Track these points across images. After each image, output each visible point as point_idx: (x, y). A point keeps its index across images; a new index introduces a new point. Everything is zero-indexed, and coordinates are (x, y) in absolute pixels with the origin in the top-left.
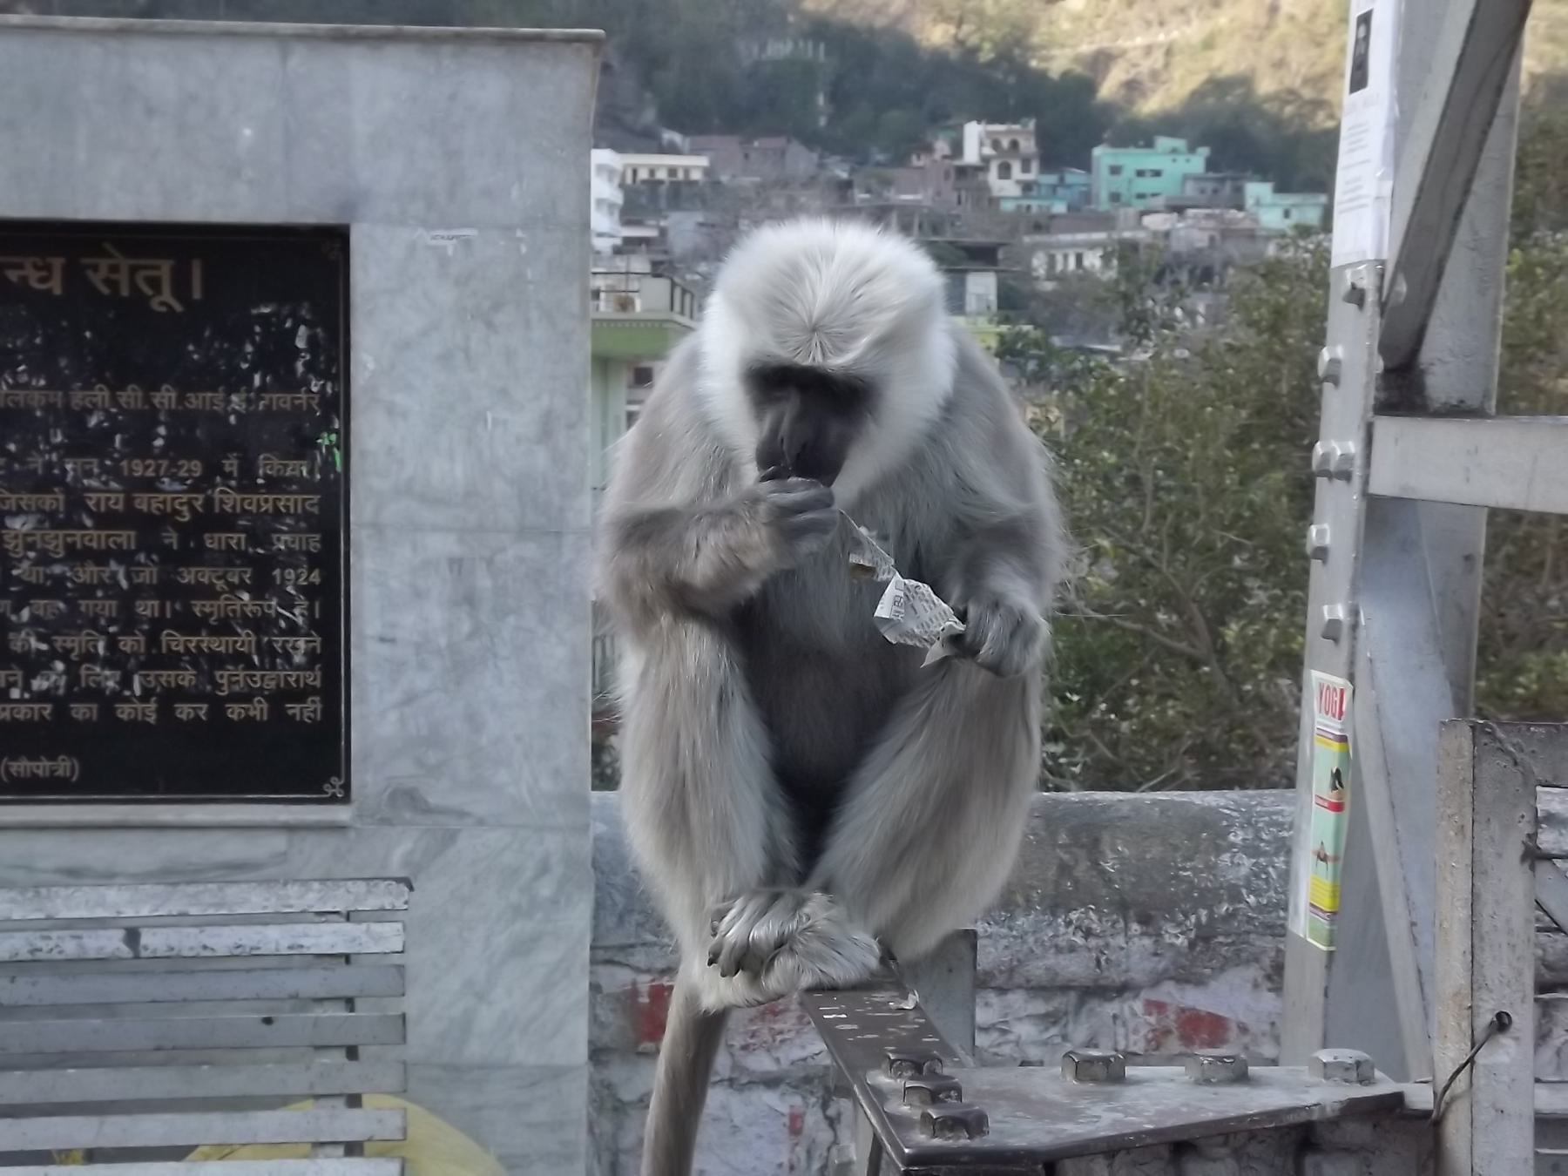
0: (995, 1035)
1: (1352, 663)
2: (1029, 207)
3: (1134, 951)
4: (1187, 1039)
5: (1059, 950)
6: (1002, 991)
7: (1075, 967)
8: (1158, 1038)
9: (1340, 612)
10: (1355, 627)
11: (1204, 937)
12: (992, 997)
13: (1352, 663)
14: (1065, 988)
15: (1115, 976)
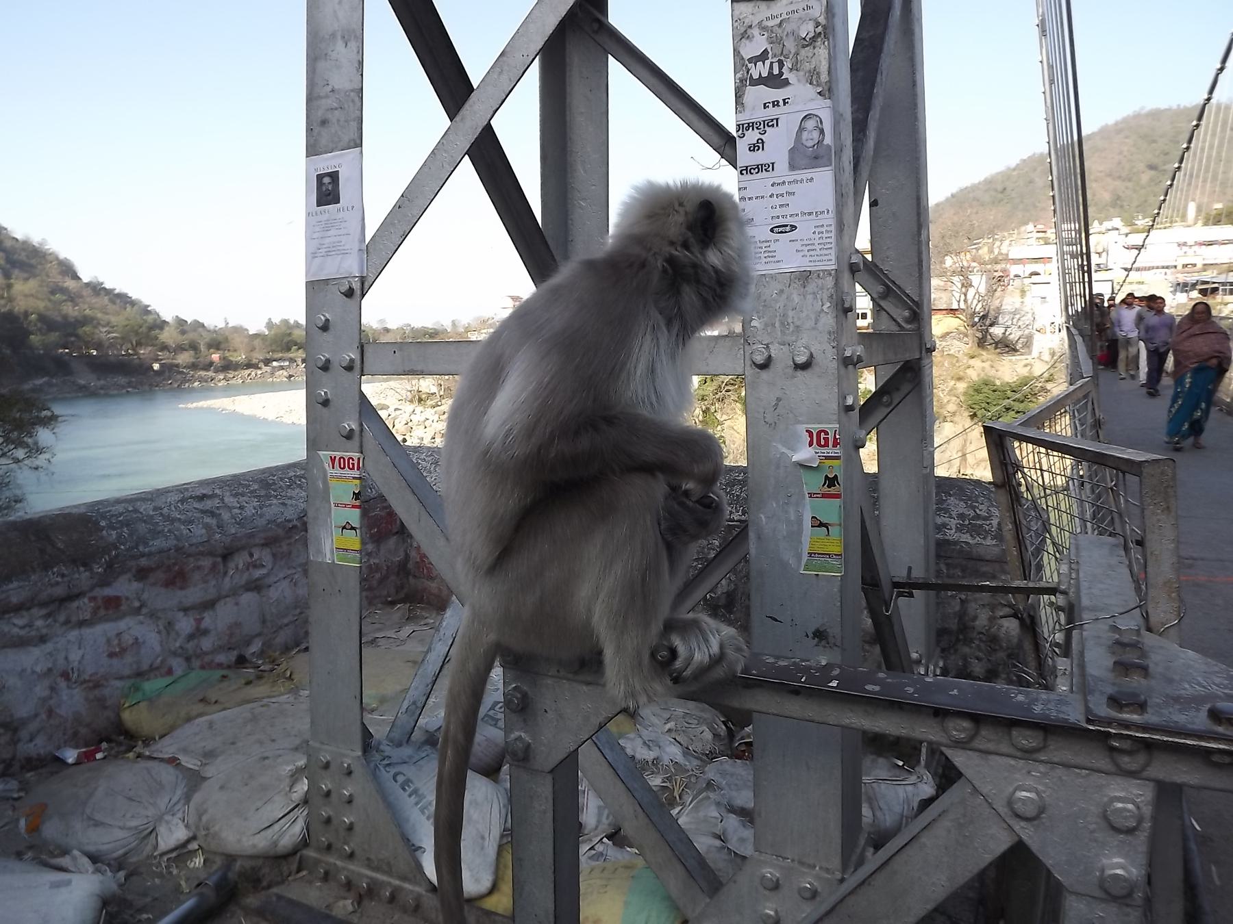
0: (27, 629)
1: (361, 446)
2: (1101, 224)
3: (83, 578)
4: (107, 608)
5: (52, 586)
6: (29, 609)
7: (59, 591)
8: (95, 611)
10: (362, 430)
11: (110, 566)
12: (25, 613)
13: (361, 446)
14: (53, 601)
15: (76, 591)
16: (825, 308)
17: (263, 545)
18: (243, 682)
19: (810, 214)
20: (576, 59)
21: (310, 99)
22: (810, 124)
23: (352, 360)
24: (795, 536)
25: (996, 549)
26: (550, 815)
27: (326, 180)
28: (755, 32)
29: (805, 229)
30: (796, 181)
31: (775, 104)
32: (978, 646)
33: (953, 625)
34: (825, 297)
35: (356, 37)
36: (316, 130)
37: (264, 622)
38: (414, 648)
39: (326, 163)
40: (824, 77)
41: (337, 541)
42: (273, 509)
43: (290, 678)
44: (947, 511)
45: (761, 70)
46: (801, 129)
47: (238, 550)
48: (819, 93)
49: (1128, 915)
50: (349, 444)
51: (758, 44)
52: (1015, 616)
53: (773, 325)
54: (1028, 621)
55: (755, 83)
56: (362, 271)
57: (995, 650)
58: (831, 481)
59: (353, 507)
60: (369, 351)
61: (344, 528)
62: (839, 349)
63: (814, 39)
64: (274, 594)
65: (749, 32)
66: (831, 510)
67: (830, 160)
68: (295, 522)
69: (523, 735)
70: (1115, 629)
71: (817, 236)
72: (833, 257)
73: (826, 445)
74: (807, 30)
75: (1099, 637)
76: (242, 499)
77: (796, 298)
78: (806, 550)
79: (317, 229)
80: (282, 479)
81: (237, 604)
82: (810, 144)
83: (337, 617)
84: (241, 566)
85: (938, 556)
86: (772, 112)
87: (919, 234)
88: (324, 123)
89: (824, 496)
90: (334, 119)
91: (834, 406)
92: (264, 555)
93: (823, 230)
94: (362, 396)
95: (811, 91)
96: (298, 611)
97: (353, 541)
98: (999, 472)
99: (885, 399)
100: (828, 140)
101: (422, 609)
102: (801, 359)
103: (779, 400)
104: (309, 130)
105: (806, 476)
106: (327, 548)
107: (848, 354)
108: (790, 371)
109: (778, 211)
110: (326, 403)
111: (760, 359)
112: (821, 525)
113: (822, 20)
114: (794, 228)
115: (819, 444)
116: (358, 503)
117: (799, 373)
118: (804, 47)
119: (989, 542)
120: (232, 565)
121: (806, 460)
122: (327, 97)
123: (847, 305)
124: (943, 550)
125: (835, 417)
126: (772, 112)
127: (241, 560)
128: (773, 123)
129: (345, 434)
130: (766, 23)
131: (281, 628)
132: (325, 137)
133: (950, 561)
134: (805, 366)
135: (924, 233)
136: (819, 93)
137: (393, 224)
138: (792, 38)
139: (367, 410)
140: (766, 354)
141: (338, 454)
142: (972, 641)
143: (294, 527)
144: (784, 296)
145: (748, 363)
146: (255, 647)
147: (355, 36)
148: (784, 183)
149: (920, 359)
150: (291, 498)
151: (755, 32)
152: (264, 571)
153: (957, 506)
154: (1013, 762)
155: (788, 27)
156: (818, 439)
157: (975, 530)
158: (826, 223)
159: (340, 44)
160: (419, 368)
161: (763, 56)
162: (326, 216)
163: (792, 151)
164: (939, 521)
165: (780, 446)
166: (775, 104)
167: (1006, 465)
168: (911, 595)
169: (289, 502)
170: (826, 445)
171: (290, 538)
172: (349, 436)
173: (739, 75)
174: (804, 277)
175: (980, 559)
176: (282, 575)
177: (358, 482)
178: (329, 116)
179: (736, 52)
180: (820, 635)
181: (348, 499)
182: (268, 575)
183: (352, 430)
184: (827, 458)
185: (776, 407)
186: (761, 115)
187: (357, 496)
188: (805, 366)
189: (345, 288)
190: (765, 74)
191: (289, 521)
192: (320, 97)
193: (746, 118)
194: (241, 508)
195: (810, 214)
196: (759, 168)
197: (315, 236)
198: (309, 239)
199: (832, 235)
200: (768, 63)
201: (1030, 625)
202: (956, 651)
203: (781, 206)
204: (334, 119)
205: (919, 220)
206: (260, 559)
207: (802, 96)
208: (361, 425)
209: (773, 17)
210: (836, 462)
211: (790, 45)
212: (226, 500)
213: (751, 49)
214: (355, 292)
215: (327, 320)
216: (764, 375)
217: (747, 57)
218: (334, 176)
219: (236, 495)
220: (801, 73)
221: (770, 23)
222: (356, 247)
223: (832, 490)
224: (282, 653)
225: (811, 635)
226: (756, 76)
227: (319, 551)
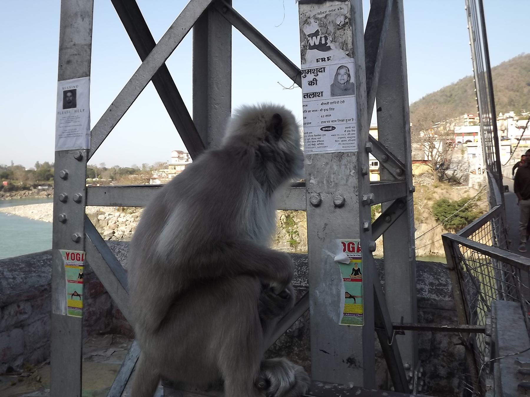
10: (85, 238)
16: (352, 173)
17: (26, 300)
18: (10, 383)
19: (343, 121)
20: (214, 27)
21: (61, 49)
22: (342, 71)
23: (80, 197)
24: (336, 304)
25: (451, 304)
27: (69, 94)
28: (312, 20)
29: (340, 129)
30: (335, 102)
31: (323, 60)
32: (443, 359)
33: (428, 347)
34: (352, 167)
35: (88, 15)
36: (64, 66)
37: (25, 346)
38: (114, 362)
39: (69, 85)
40: (350, 46)
41: (69, 301)
42: (33, 279)
43: (39, 381)
44: (423, 281)
45: (315, 41)
46: (337, 74)
47: (11, 303)
50: (77, 245)
51: (313, 27)
52: (462, 344)
53: (322, 182)
54: (469, 347)
55: (311, 48)
56: (88, 146)
57: (452, 361)
58: (356, 272)
59: (79, 282)
60: (90, 192)
61: (73, 295)
62: (360, 196)
63: (344, 25)
64: (31, 329)
65: (309, 20)
66: (356, 289)
67: (354, 91)
68: (46, 287)
70: (518, 363)
72: (356, 145)
73: (353, 251)
74: (340, 20)
75: (509, 368)
76: (14, 273)
77: (335, 168)
78: (342, 310)
79: (63, 121)
80: (39, 261)
81: (9, 336)
82: (342, 82)
83: (67, 348)
84: (12, 313)
85: (419, 307)
86: (321, 64)
87: (405, 128)
88: (69, 62)
89: (353, 280)
90: (74, 61)
91: (357, 228)
92: (26, 306)
93: (350, 129)
94: (86, 217)
95: (342, 53)
96: (46, 340)
97: (78, 302)
98: (451, 262)
99: (387, 218)
100: (352, 80)
101: (120, 337)
102: (338, 202)
103: (326, 225)
104: (60, 66)
105: (342, 268)
106: (63, 306)
107: (365, 198)
108: (332, 208)
110: (64, 221)
111: (315, 201)
112: (351, 297)
113: (348, 15)
114: (334, 128)
115: (349, 250)
116: (81, 280)
117: (338, 210)
118: (339, 29)
119: (447, 299)
120: (7, 312)
121: (343, 260)
122: (71, 48)
123: (364, 171)
124: (420, 303)
125: (358, 235)
126: (321, 64)
127: (12, 309)
128: (322, 70)
129: (75, 239)
130: (317, 16)
131: (35, 350)
133: (425, 310)
134: (341, 206)
135: (407, 126)
137: (106, 120)
138: (332, 25)
139: (88, 225)
141: (71, 251)
142: (439, 355)
143: (46, 289)
144: (329, 166)
145: (308, 203)
146: (19, 362)
147: (88, 15)
148: (328, 103)
149: (406, 196)
150: (44, 272)
151: (312, 20)
152: (26, 316)
153: (428, 278)
155: (330, 19)
156: (348, 247)
157: (439, 292)
158: (351, 126)
159: (79, 20)
161: (316, 34)
163: (332, 86)
164: (419, 287)
165: (327, 251)
166: (323, 60)
167: (455, 257)
168: (403, 333)
169: (43, 275)
170: (353, 251)
171: (42, 296)
172: (78, 241)
173: (303, 44)
174: (340, 156)
175: (443, 309)
176: (37, 318)
177: (82, 268)
178: (72, 58)
179: (301, 31)
180: (351, 361)
181: (76, 278)
182: (29, 318)
183: (79, 238)
184: (354, 258)
186: (315, 65)
187: (81, 276)
188: (341, 206)
190: (317, 43)
191: (42, 286)
192: (67, 48)
194: (14, 278)
195: (343, 121)
196: (314, 95)
198: (58, 127)
199: (355, 132)
200: (319, 37)
201: (471, 348)
202: (430, 362)
203: (326, 116)
204: (74, 61)
205: (404, 120)
206: (24, 309)
207: (338, 57)
208: (85, 235)
209: (321, 13)
210: (359, 261)
211: (331, 28)
212: (5, 273)
213: (310, 29)
214: (83, 157)
215: (67, 174)
216: (318, 210)
217: (307, 34)
218: (74, 92)
219: (11, 271)
220: (337, 44)
222: (85, 132)
223: (357, 277)
224: (36, 365)
225: (345, 361)
226: (312, 44)
227: (58, 308)
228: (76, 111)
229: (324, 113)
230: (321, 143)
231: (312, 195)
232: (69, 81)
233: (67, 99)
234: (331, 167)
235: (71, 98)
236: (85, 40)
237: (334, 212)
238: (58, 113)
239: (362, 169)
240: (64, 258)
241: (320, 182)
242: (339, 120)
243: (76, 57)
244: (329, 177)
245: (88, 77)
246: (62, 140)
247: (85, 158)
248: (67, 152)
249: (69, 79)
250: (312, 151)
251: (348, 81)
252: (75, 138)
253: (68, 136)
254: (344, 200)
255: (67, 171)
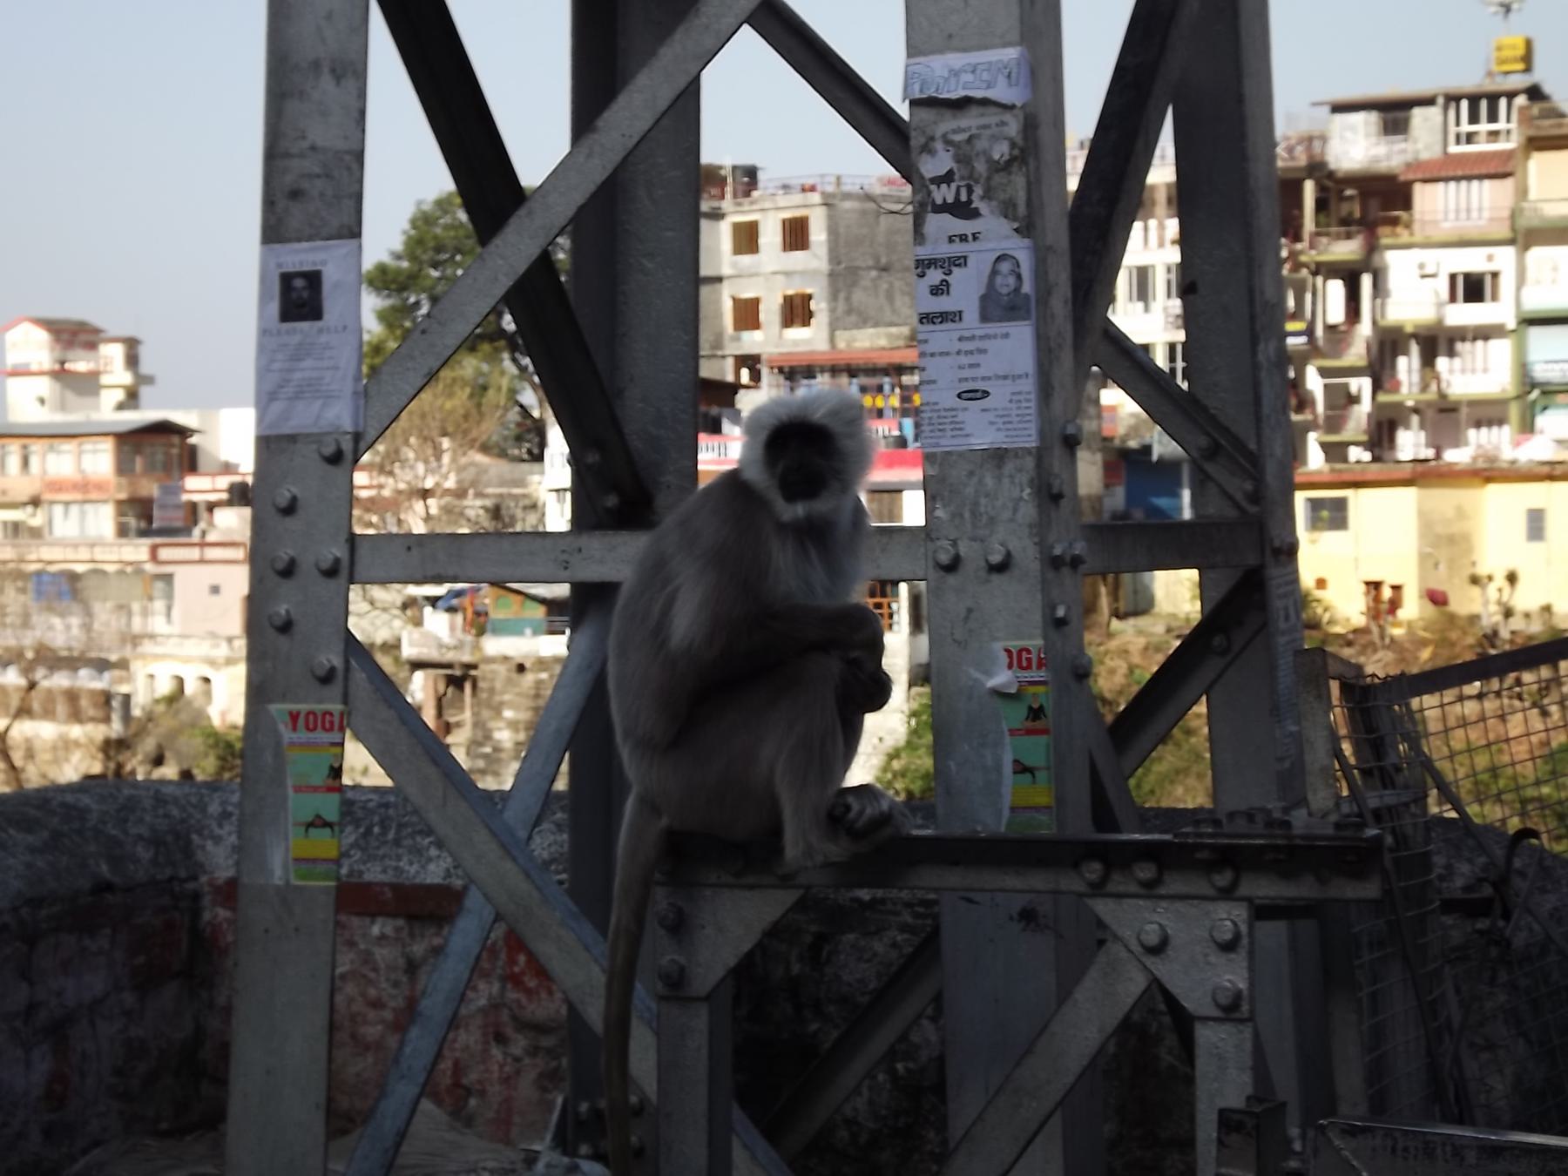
9: (337, 662)
10: (347, 669)
19: (1005, 377)
22: (1005, 267)
26: (705, 1051)
27: (299, 283)
29: (1000, 395)
36: (282, 204)
39: (299, 257)
40: (1022, 210)
45: (943, 194)
46: (994, 273)
48: (1016, 230)
49: (1241, 1032)
53: (961, 516)
55: (939, 209)
56: (356, 423)
58: (1036, 713)
61: (310, 825)
62: (1043, 545)
63: (1009, 163)
66: (1036, 750)
67: (1028, 311)
69: (676, 957)
71: (1014, 405)
74: (1001, 151)
77: (989, 481)
78: (1007, 801)
79: (280, 356)
82: (1005, 291)
86: (958, 248)
88: (296, 194)
89: (1029, 732)
91: (1037, 617)
93: (1021, 397)
95: (1005, 226)
99: (1218, 640)
100: (1027, 288)
102: (996, 558)
103: (970, 611)
104: (269, 203)
107: (1058, 551)
108: (983, 574)
109: (967, 373)
110: (286, 627)
111: (944, 558)
114: (986, 394)
117: (995, 578)
118: (997, 171)
121: (1004, 685)
122: (302, 156)
123: (1055, 491)
125: (1039, 632)
126: (958, 248)
128: (961, 261)
132: (297, 215)
134: (1001, 568)
135: (1266, 351)
136: (1016, 230)
138: (982, 159)
140: (952, 551)
141: (303, 707)
144: (975, 479)
145: (931, 563)
147: (353, 71)
154: (1141, 902)
156: (1018, 659)
159: (327, 82)
160: (451, 572)
161: (948, 178)
162: (296, 339)
170: (1029, 667)
172: (327, 678)
174: (998, 456)
178: (305, 185)
185: (967, 618)
186: (945, 250)
188: (1001, 568)
189: (329, 450)
190: (950, 200)
192: (288, 155)
193: (924, 252)
195: (1005, 377)
196: (944, 317)
197: (276, 366)
200: (954, 186)
203: (971, 366)
207: (995, 235)
208: (347, 662)
210: (1041, 689)
211: (981, 167)
216: (952, 580)
218: (313, 279)
220: (994, 203)
221: (958, 138)
223: (1038, 724)
225: (1015, 916)
226: (939, 201)
228: (321, 331)
229: (965, 360)
230: (958, 427)
231: (939, 543)
232: (296, 246)
233: (294, 295)
234: (980, 482)
235: (305, 294)
236: (346, 138)
237: (988, 581)
238: (264, 332)
239: (1050, 486)
240: (282, 728)
241: (957, 515)
242: (998, 377)
243: (319, 183)
244: (976, 504)
245: (354, 242)
246: (277, 407)
247: (349, 456)
248: (292, 438)
249: (299, 240)
250: (937, 445)
251: (1017, 290)
252: (319, 403)
253: (297, 396)
254: (1008, 555)
255: (295, 490)
